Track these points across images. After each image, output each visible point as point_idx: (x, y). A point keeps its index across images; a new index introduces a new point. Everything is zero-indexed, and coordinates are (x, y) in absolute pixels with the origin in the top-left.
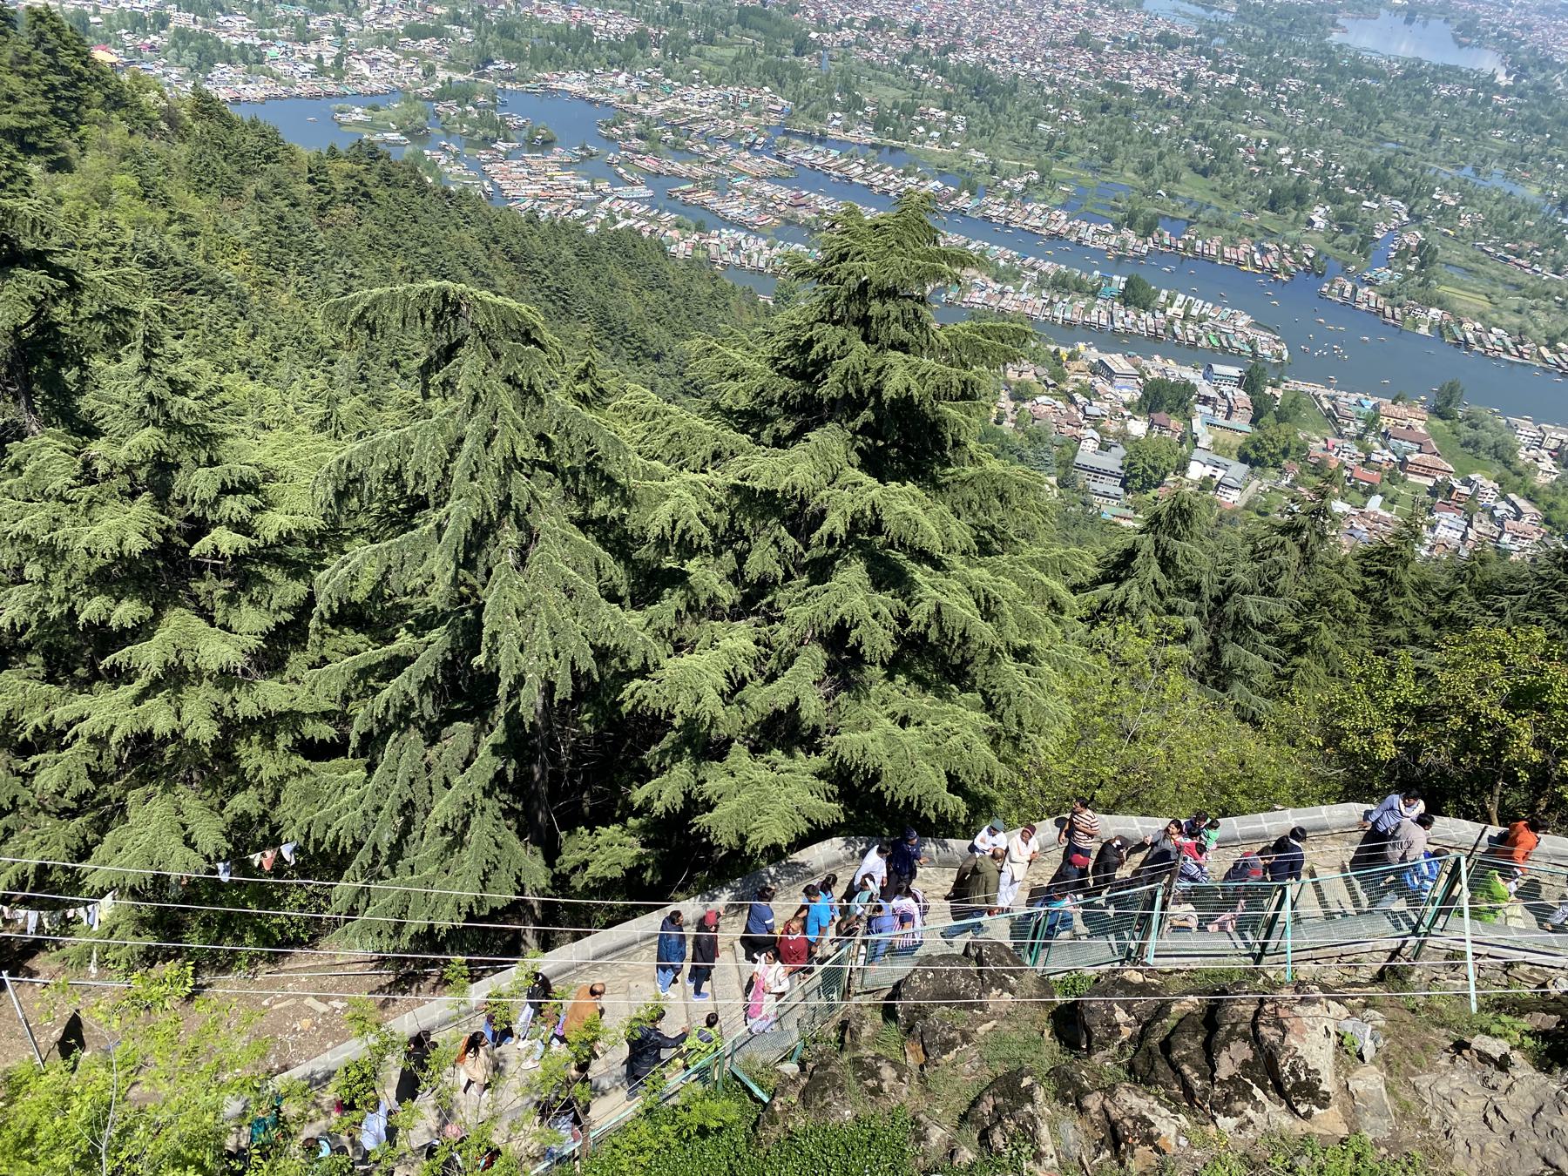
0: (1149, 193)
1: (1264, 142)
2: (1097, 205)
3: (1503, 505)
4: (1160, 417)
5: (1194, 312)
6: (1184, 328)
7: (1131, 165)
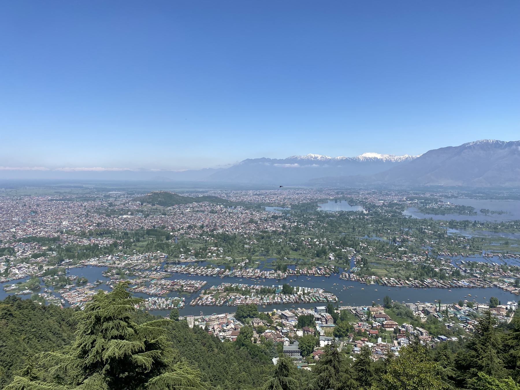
0: (282, 259)
2: (268, 266)
3: (415, 331)
4: (306, 328)
5: (306, 292)
6: (304, 297)
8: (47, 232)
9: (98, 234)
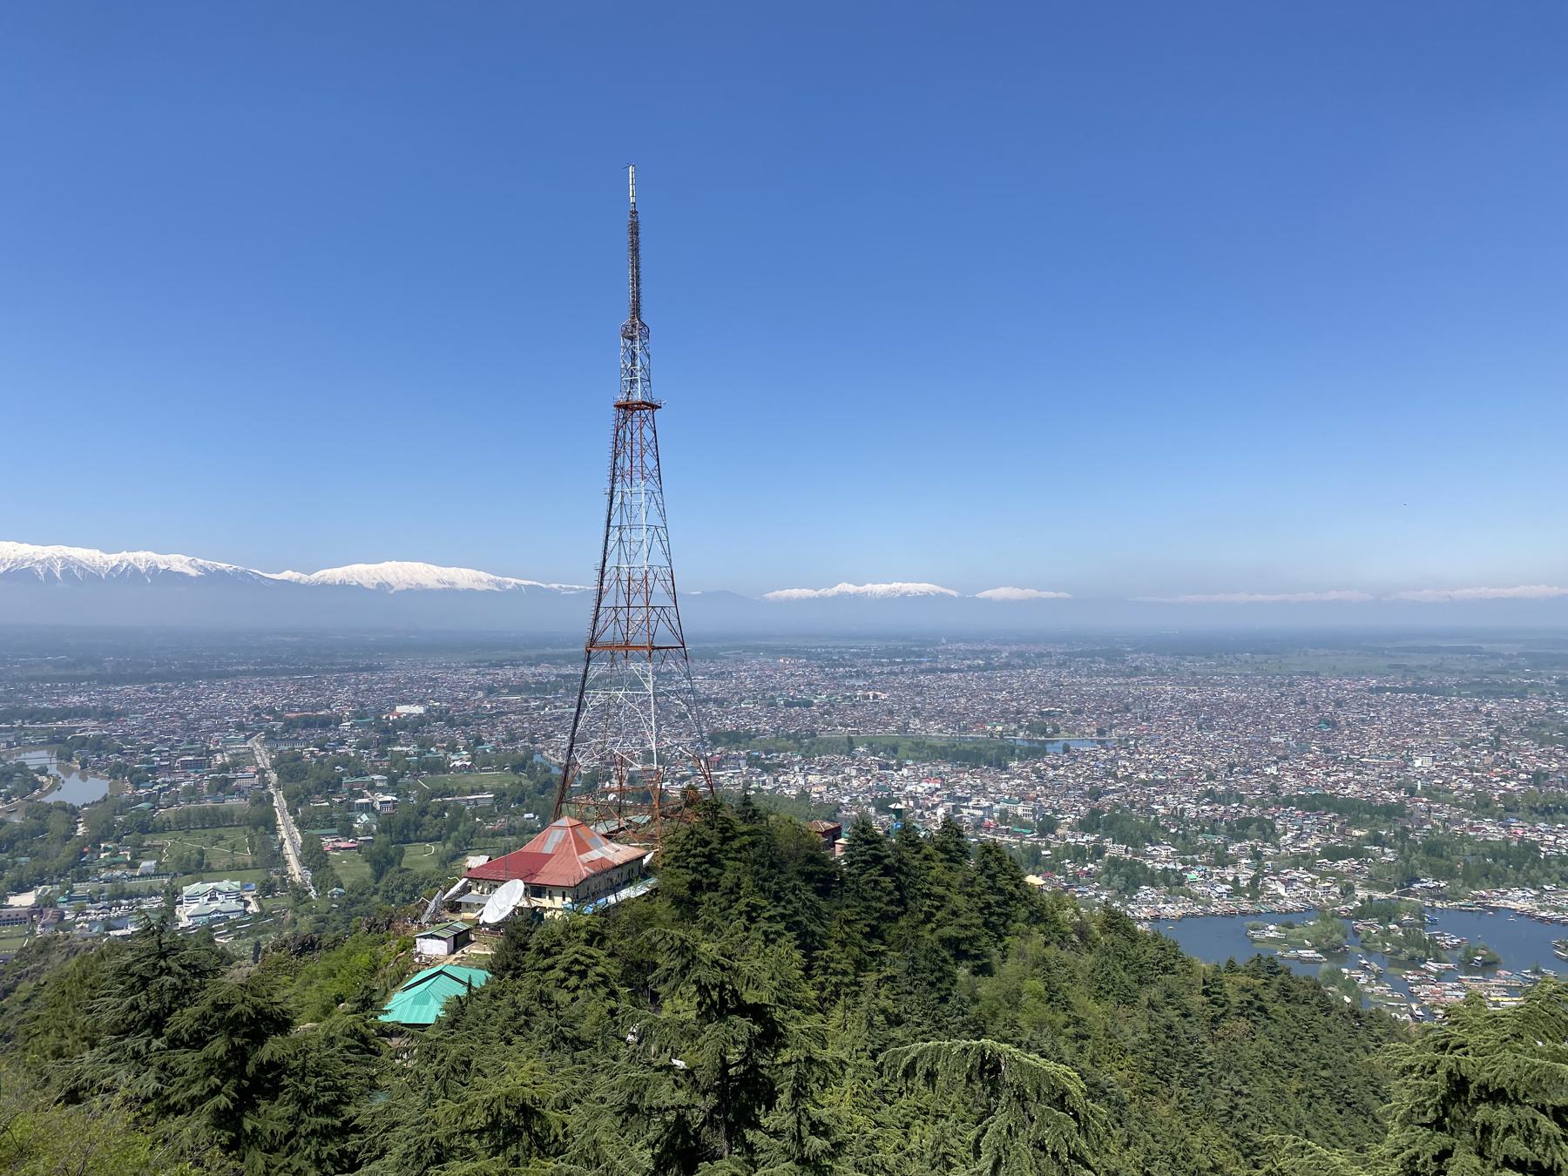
8: (1365, 786)
9: (1536, 810)
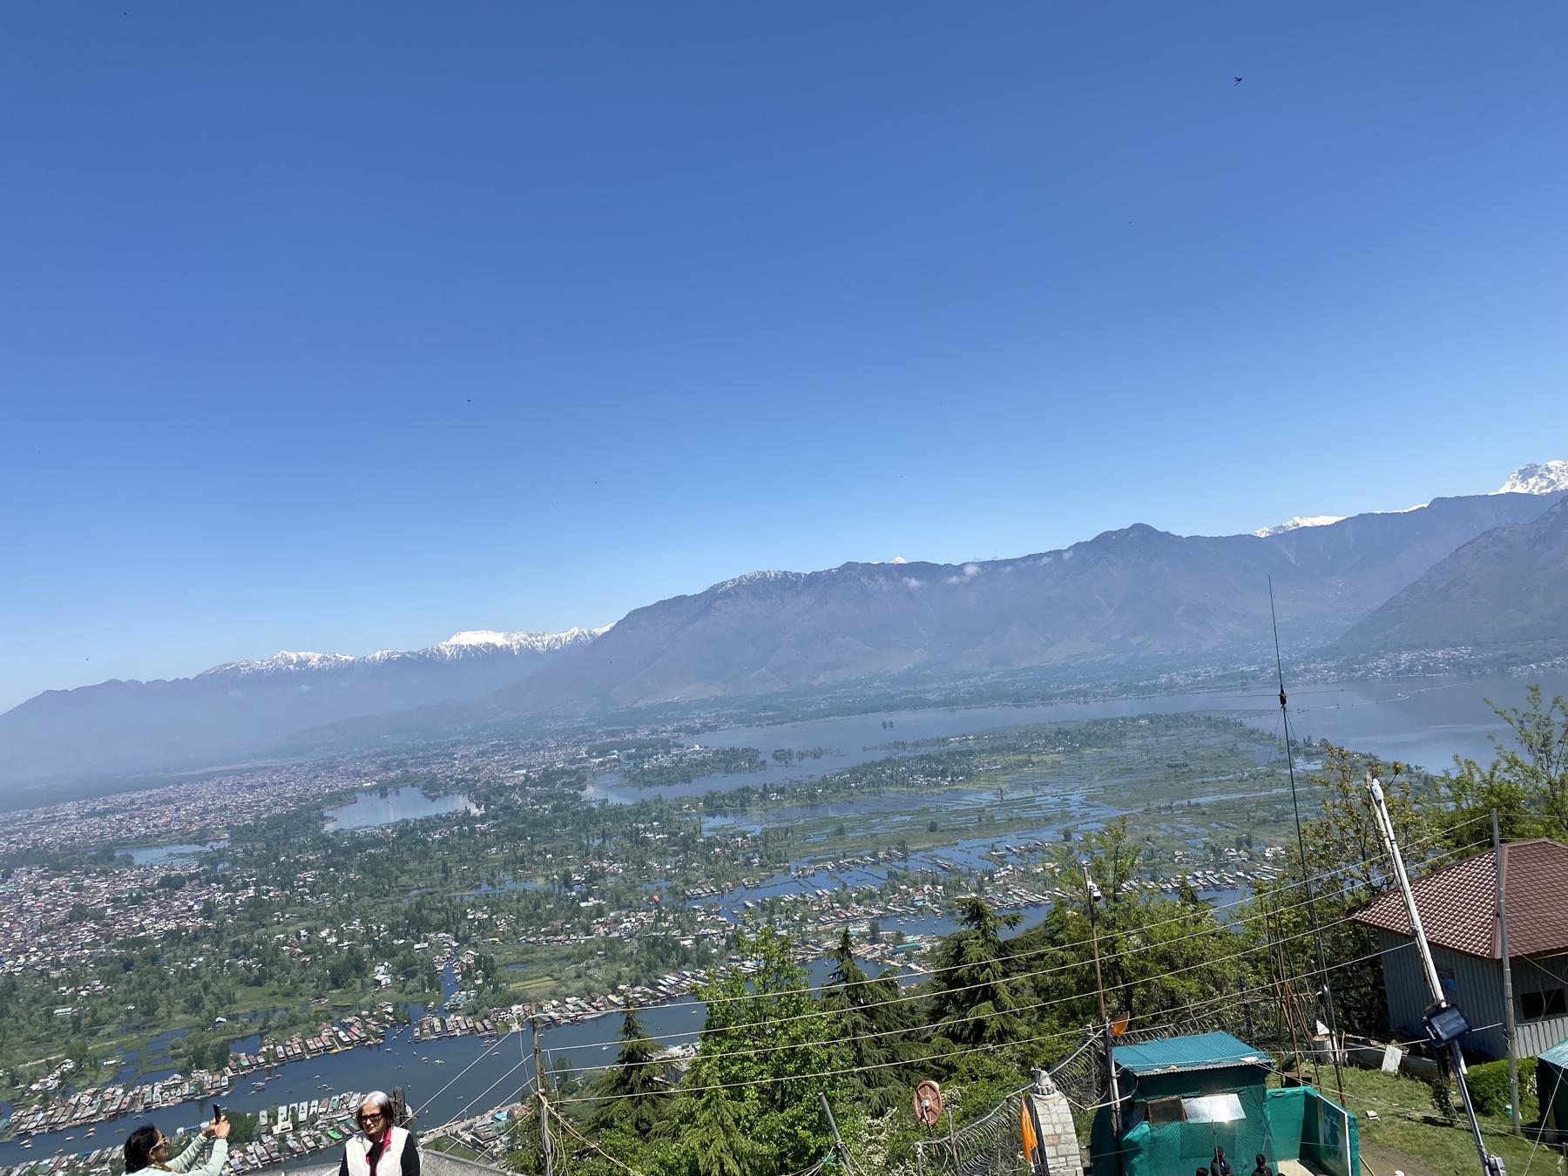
1: (303, 932)
7: (178, 1008)
